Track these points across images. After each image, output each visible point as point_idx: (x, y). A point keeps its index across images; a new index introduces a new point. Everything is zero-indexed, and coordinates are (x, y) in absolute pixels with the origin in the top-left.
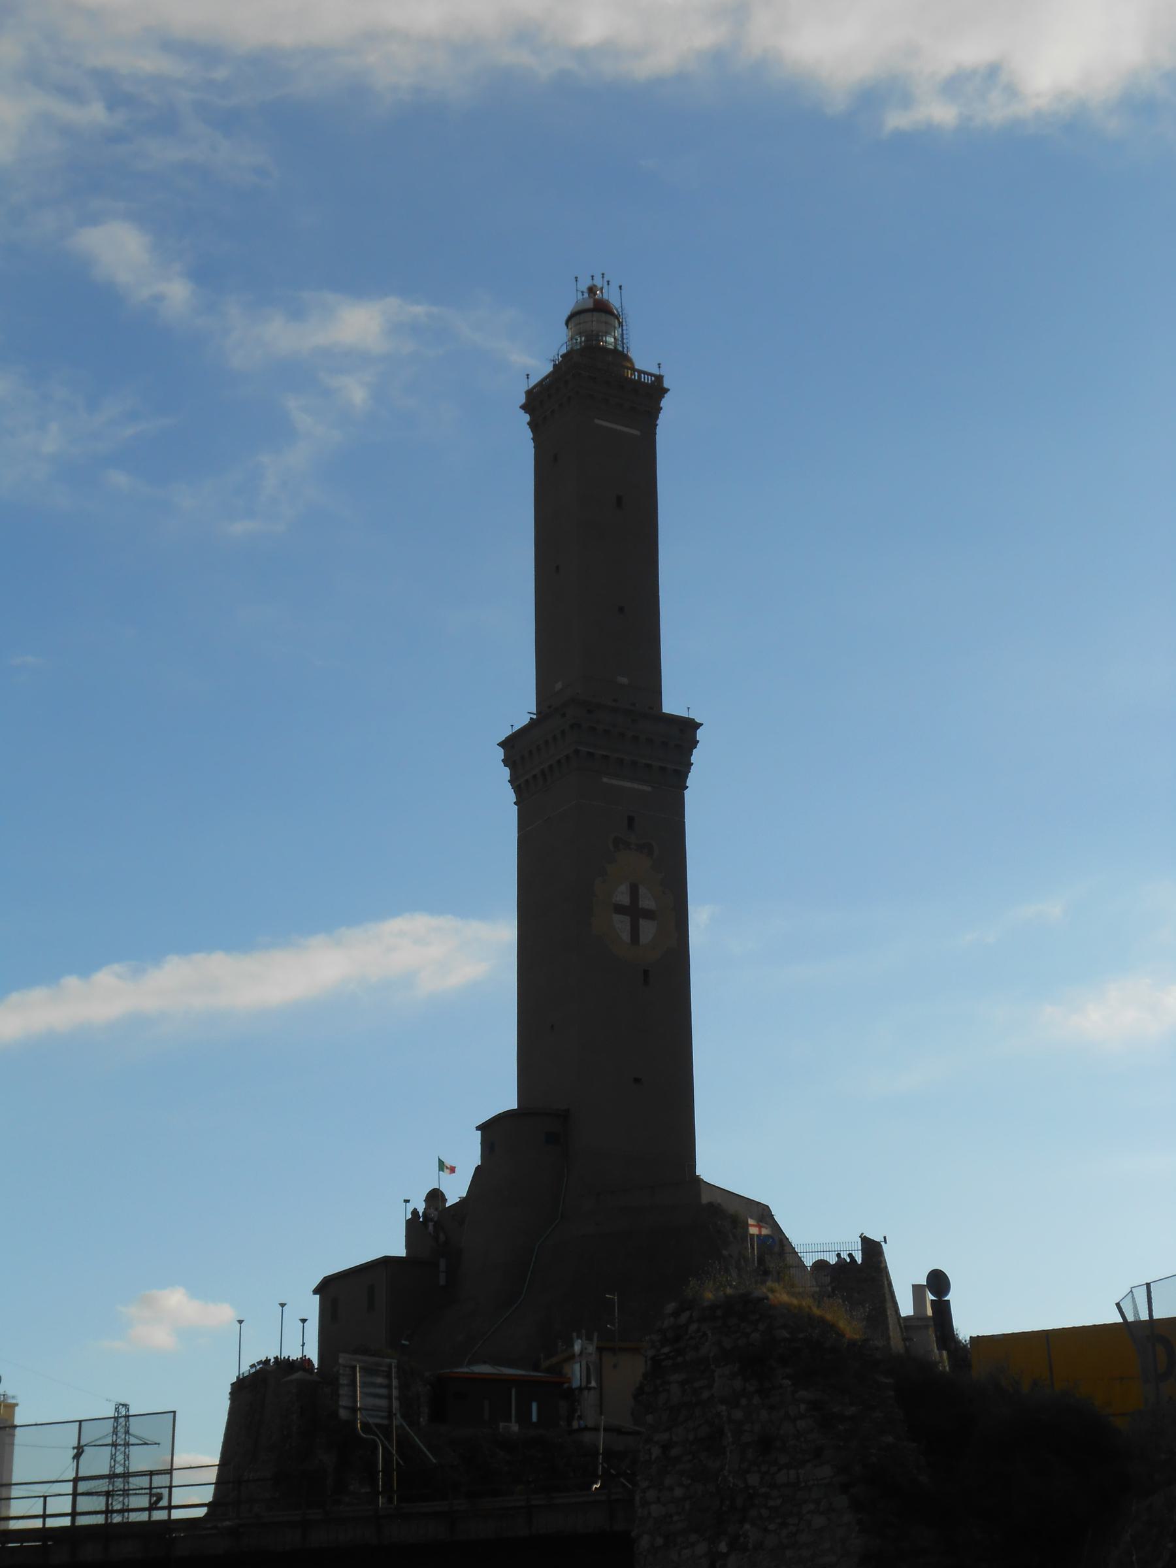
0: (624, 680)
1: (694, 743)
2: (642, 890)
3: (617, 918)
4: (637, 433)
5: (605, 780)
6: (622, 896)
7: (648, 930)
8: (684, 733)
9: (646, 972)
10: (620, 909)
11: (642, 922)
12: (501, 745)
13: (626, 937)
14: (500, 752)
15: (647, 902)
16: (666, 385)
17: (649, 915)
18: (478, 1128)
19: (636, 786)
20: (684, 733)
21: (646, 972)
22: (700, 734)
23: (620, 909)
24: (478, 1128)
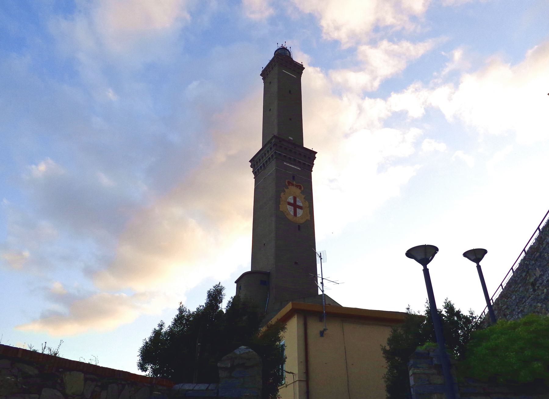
0: (292, 138)
2: (297, 199)
3: (288, 206)
7: (300, 212)
8: (311, 155)
9: (299, 226)
10: (289, 204)
13: (292, 213)
14: (250, 164)
15: (299, 203)
17: (301, 208)
18: (235, 282)
21: (299, 226)
22: (316, 155)
23: (289, 204)
24: (235, 282)
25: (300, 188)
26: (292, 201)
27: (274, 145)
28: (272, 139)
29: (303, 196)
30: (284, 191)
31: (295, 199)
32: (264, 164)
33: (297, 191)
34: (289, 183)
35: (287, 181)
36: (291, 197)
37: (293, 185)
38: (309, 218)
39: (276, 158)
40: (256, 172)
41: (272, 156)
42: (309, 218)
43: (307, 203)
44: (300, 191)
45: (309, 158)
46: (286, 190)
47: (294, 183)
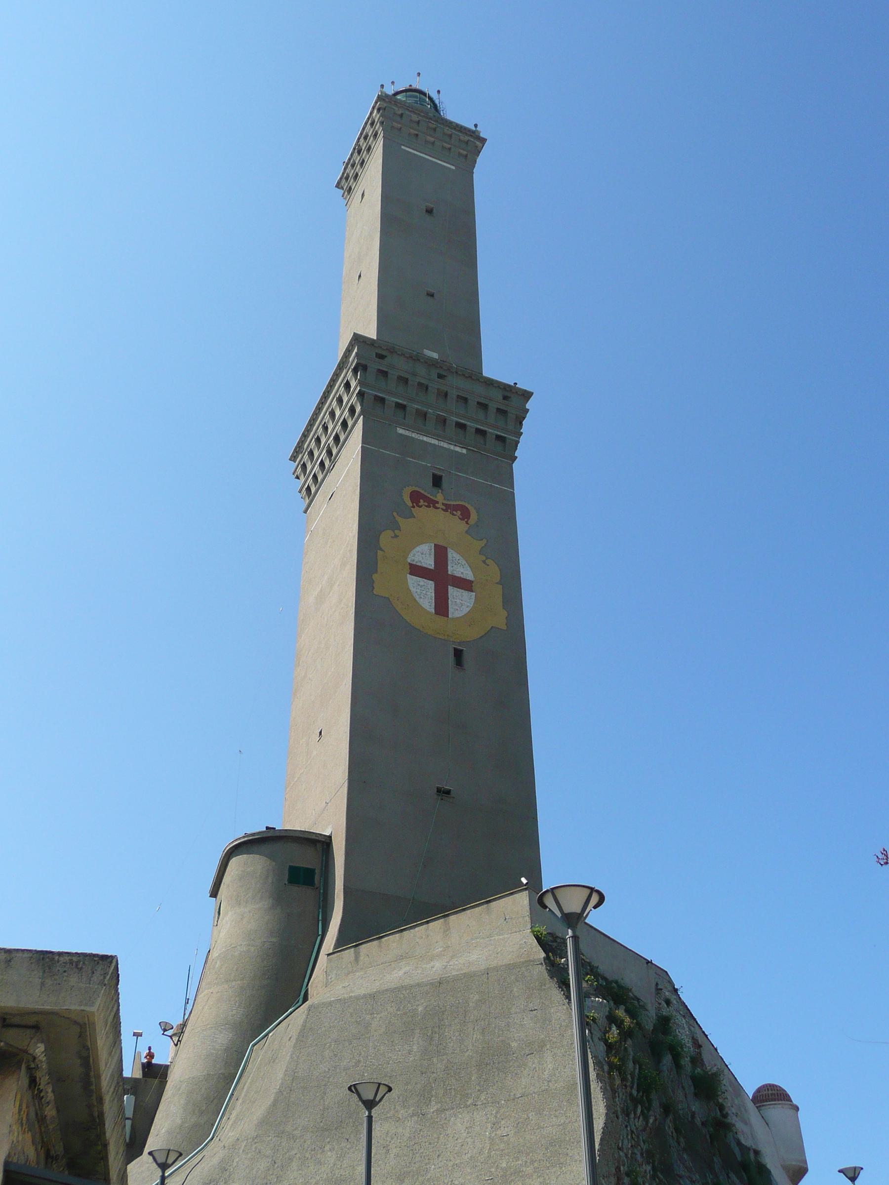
0: (435, 355)
2: (452, 555)
4: (453, 168)
5: (400, 431)
6: (424, 556)
10: (417, 571)
11: (451, 589)
16: (482, 135)
17: (465, 585)
19: (445, 445)
20: (511, 403)
21: (458, 654)
23: (417, 571)
25: (465, 515)
26: (429, 562)
27: (355, 371)
30: (395, 526)
31: (441, 554)
32: (330, 453)
34: (416, 497)
35: (407, 492)
37: (432, 503)
39: (363, 412)
41: (352, 410)
42: (500, 619)
43: (494, 572)
44: (462, 526)
45: (502, 412)
47: (440, 497)
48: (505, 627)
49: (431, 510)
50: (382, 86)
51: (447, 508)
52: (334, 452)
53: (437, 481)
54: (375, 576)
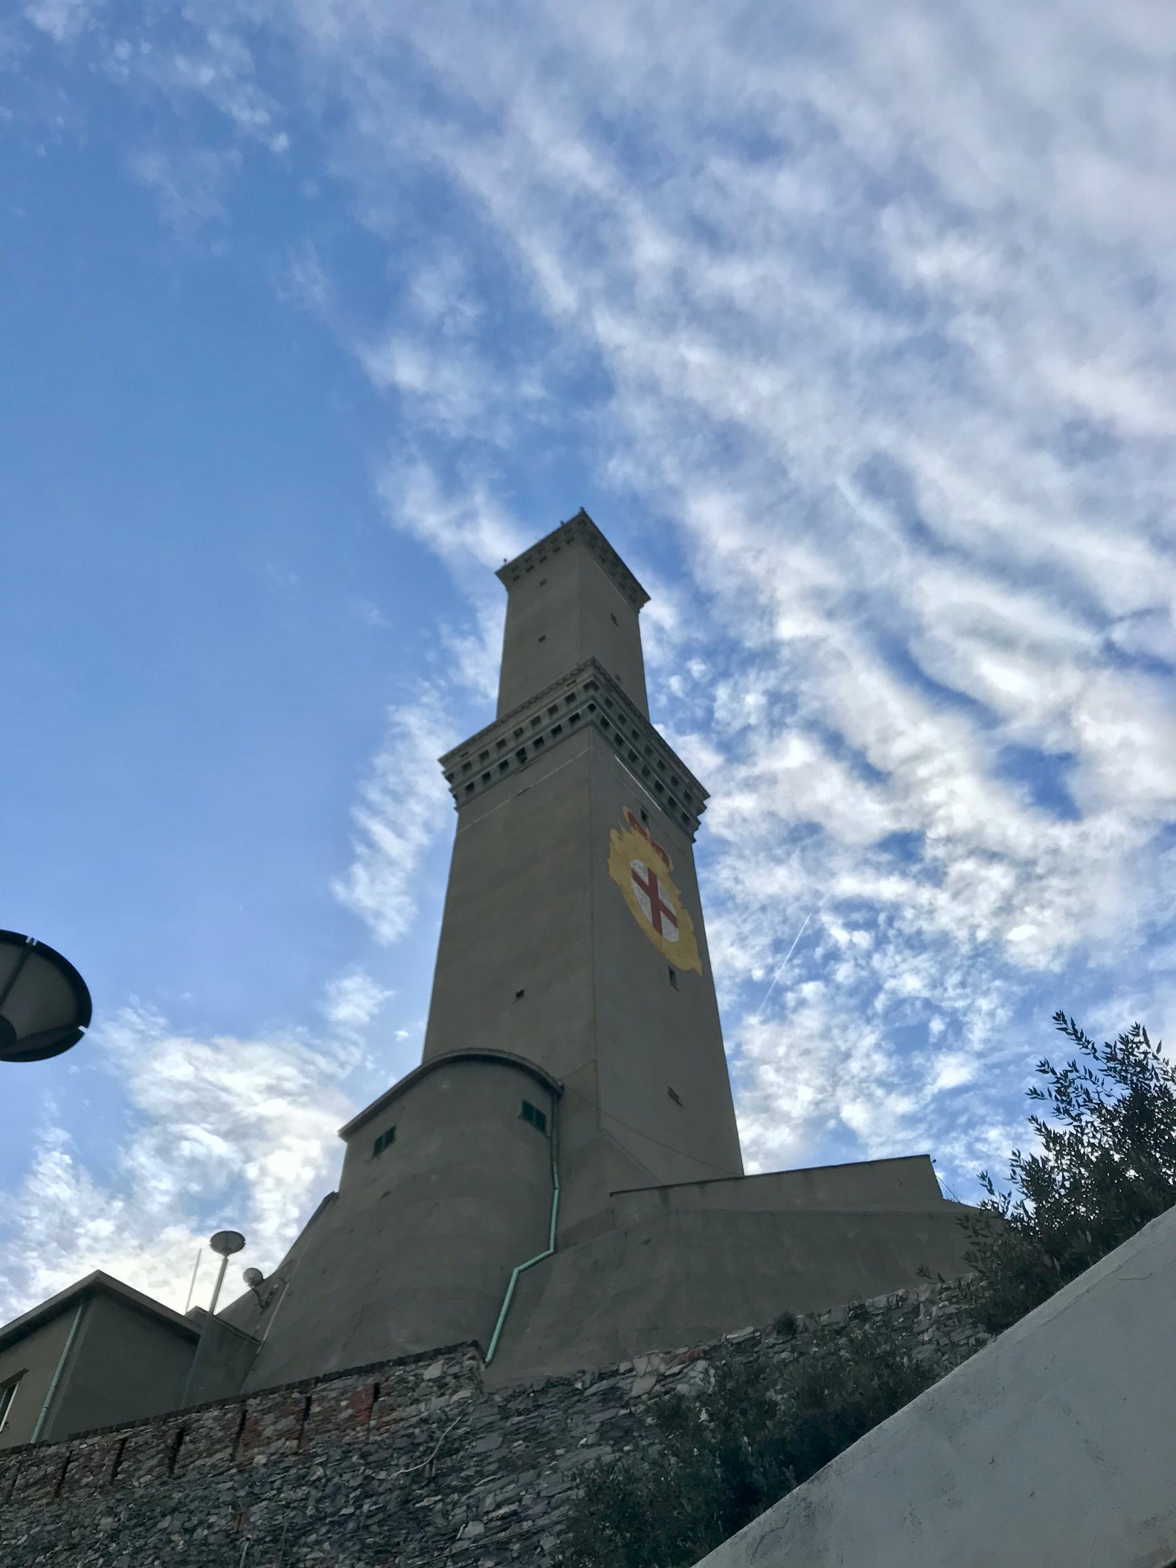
1: (702, 809)
3: (635, 885)
9: (672, 973)
11: (662, 914)
12: (443, 761)
21: (672, 973)
25: (665, 859)
26: (646, 879)
28: (580, 670)
29: (678, 892)
30: (620, 832)
31: (652, 876)
32: (521, 754)
33: (660, 868)
35: (626, 810)
36: (642, 864)
38: (698, 966)
40: (471, 787)
42: (698, 966)
45: (687, 796)
46: (624, 830)
47: (647, 830)
48: (701, 974)
49: (643, 839)
50: (582, 509)
51: (653, 845)
52: (530, 755)
53: (644, 817)
54: (610, 861)
